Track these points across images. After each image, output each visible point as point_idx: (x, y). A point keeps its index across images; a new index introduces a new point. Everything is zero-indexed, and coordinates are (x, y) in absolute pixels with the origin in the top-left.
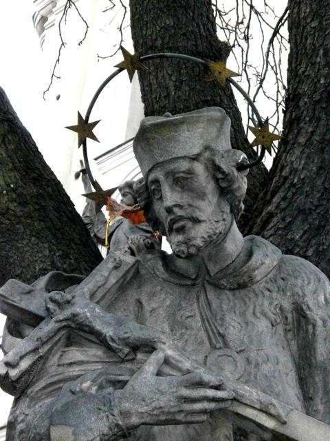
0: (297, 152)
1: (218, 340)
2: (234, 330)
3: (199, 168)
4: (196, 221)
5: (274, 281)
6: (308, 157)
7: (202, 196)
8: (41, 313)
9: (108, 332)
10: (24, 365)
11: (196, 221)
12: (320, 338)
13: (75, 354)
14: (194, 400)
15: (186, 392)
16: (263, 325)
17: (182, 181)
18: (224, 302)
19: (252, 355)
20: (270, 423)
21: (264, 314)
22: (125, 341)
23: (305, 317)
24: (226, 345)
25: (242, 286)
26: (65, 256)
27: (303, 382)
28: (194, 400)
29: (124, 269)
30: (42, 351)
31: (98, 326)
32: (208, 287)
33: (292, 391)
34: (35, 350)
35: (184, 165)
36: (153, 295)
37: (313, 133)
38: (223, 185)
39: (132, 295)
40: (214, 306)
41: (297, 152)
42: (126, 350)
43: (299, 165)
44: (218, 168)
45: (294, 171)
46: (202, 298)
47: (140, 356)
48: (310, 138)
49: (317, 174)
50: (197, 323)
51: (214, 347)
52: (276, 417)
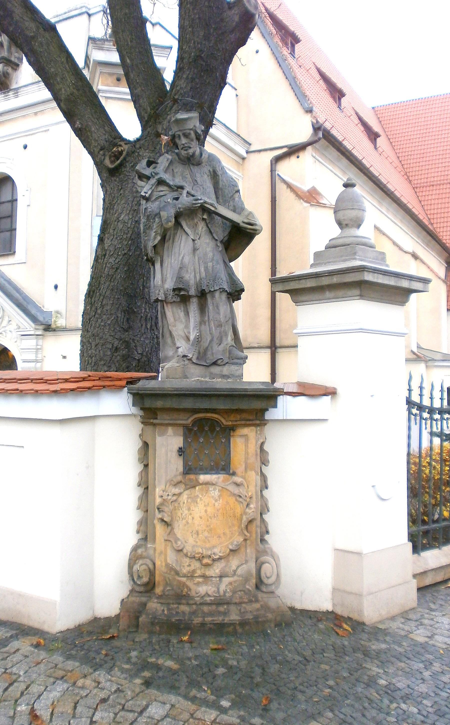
0: (183, 81)
1: (195, 182)
2: (199, 180)
3: (192, 132)
4: (190, 148)
5: (207, 162)
6: (187, 83)
7: (192, 140)
8: (150, 175)
9: (171, 183)
10: (149, 193)
11: (190, 148)
12: (220, 181)
13: (161, 188)
14: (196, 204)
15: (194, 202)
16: (206, 176)
17: (186, 136)
18: (195, 169)
19: (204, 187)
20: (213, 209)
21: (206, 174)
22: (175, 186)
23: (216, 173)
24: (198, 184)
25: (200, 164)
26: (96, 112)
27: (216, 193)
28: (196, 204)
29: (170, 161)
30: (153, 188)
31: (168, 181)
32: (190, 165)
33: (214, 196)
34: (151, 188)
35: (188, 131)
36: (176, 167)
37: (189, 74)
38: (198, 137)
39: (171, 168)
40: (193, 170)
41: (183, 81)
42: (176, 188)
43: (183, 86)
44: (198, 133)
45: (181, 88)
46: (189, 168)
47: (179, 190)
48: (188, 76)
49: (190, 90)
50: (189, 176)
51: (194, 185)
52: (215, 207)
